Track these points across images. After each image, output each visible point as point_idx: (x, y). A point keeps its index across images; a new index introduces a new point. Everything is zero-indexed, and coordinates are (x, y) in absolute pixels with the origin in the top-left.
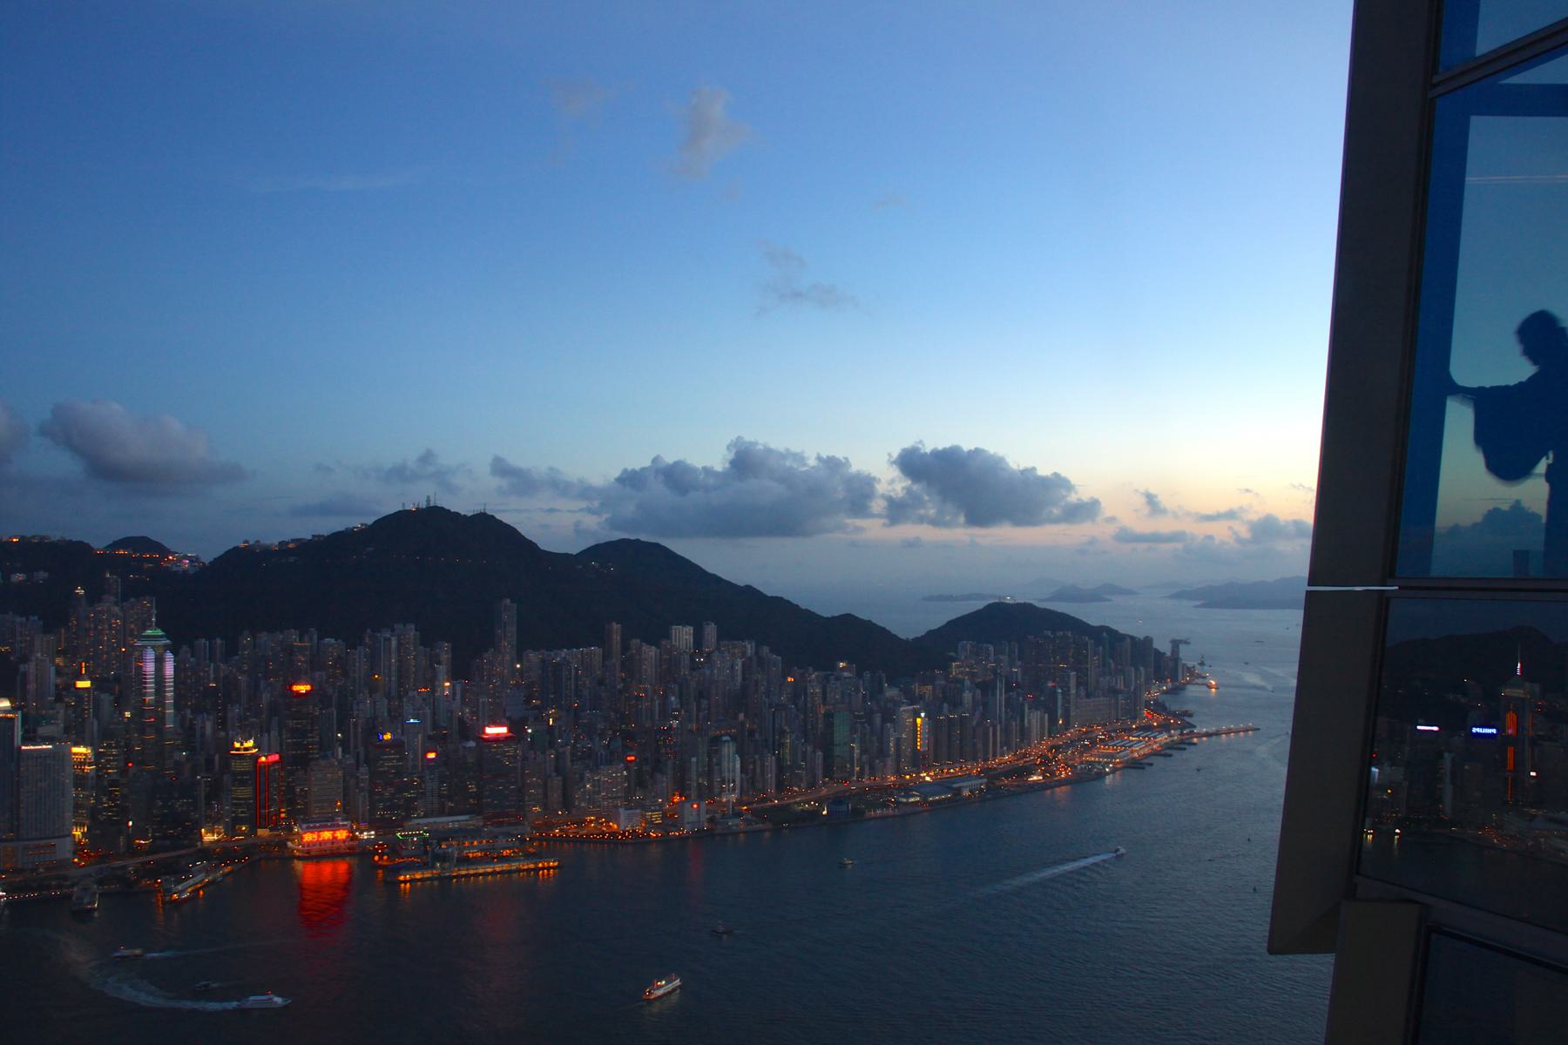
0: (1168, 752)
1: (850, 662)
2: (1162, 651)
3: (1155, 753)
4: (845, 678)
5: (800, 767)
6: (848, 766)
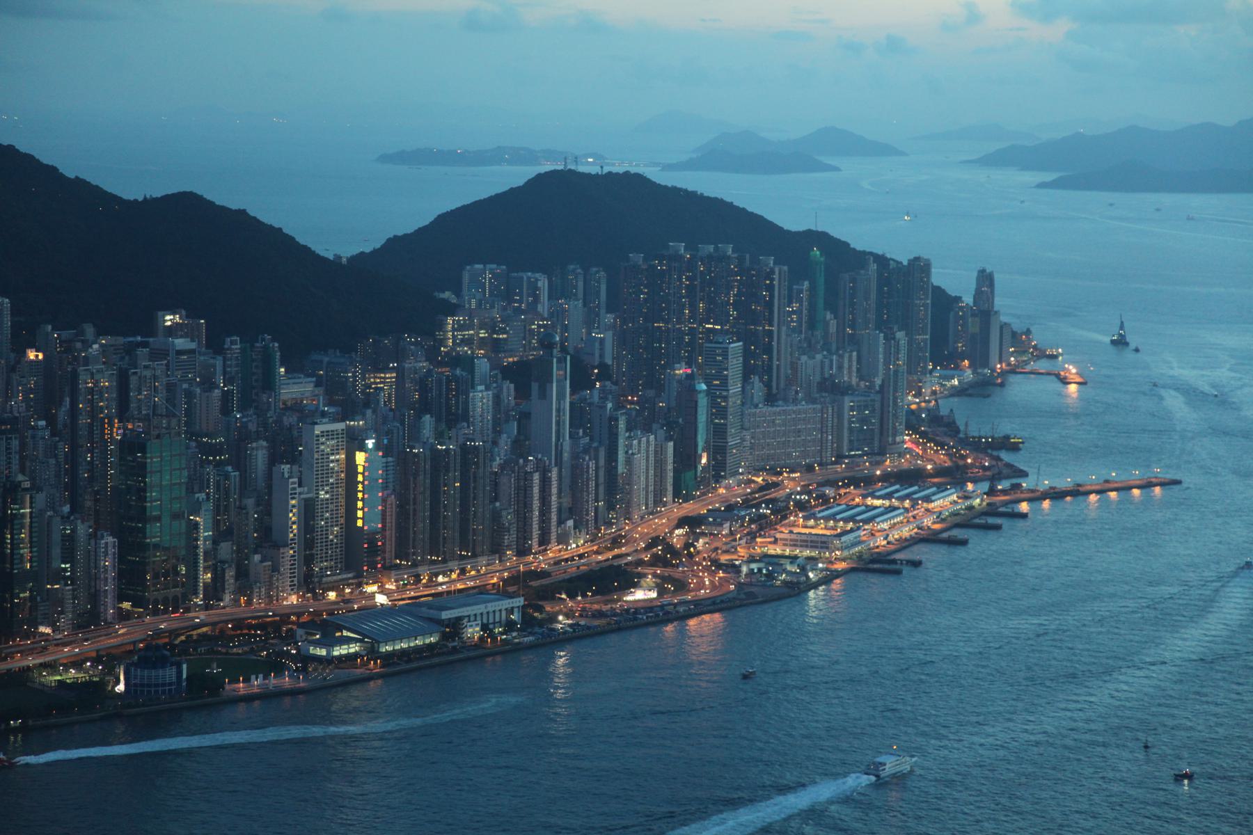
0: (958, 533)
1: (192, 313)
2: (952, 292)
3: (928, 538)
4: (180, 353)
5: (58, 576)
6: (183, 570)
